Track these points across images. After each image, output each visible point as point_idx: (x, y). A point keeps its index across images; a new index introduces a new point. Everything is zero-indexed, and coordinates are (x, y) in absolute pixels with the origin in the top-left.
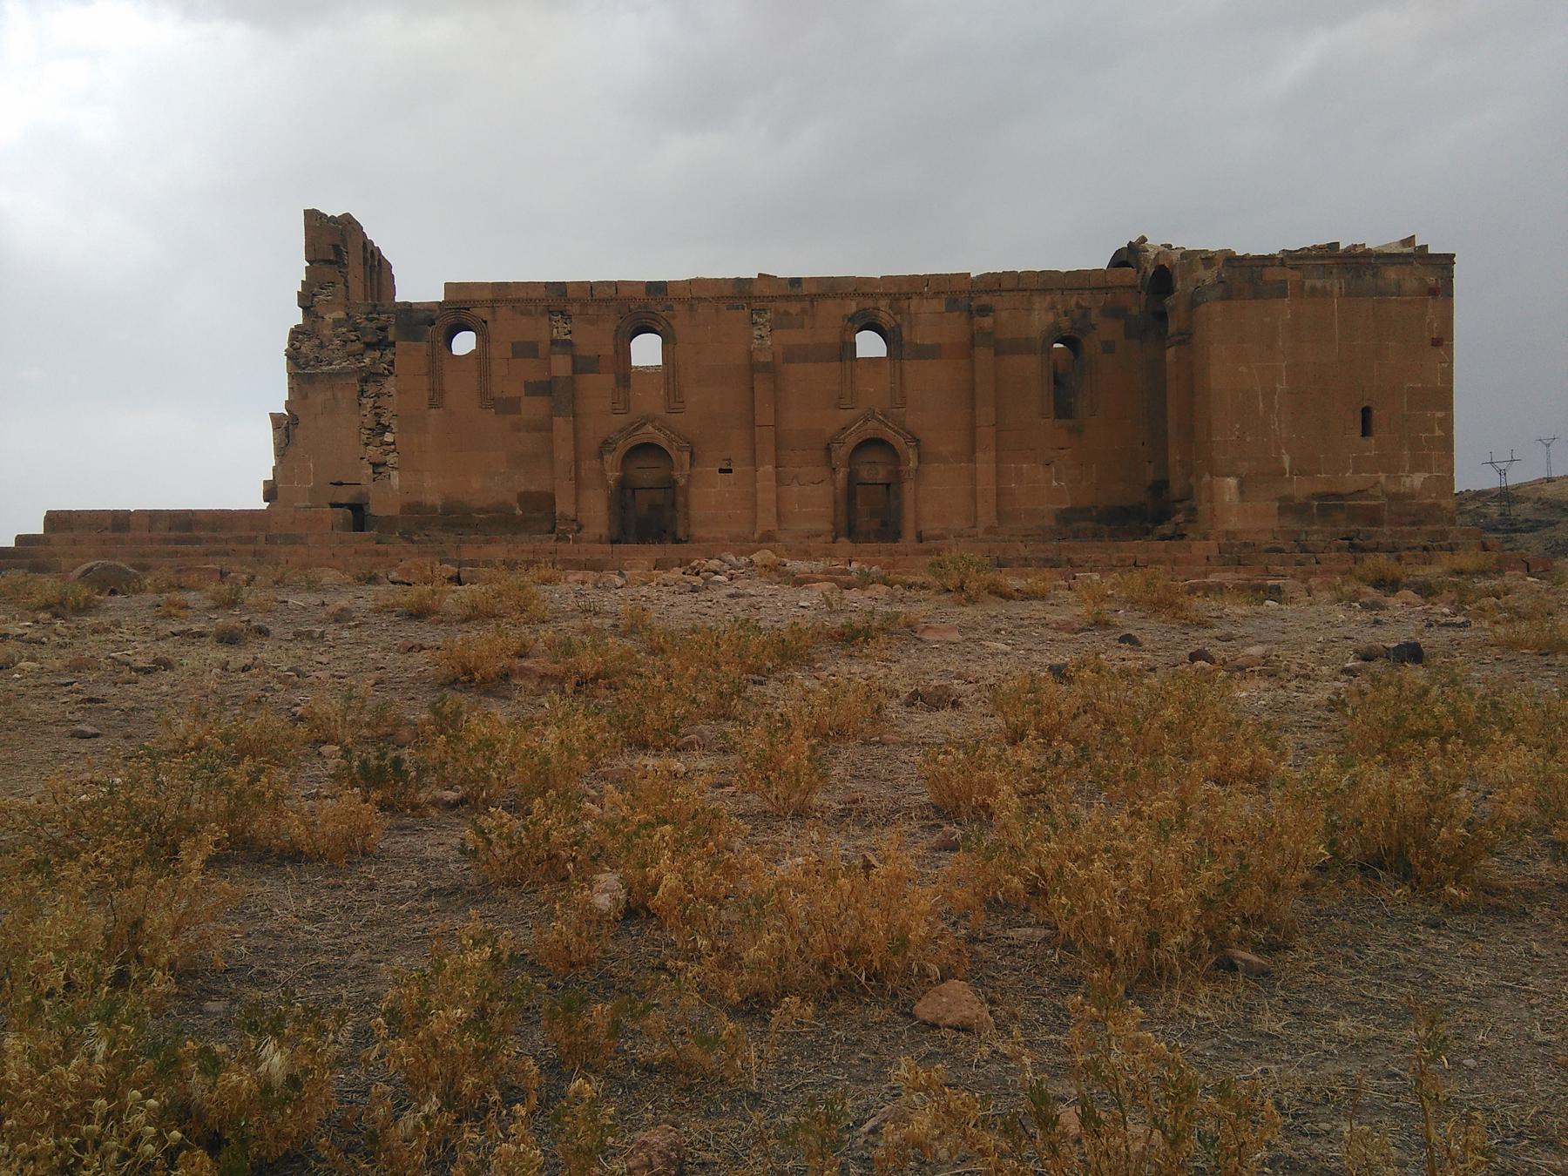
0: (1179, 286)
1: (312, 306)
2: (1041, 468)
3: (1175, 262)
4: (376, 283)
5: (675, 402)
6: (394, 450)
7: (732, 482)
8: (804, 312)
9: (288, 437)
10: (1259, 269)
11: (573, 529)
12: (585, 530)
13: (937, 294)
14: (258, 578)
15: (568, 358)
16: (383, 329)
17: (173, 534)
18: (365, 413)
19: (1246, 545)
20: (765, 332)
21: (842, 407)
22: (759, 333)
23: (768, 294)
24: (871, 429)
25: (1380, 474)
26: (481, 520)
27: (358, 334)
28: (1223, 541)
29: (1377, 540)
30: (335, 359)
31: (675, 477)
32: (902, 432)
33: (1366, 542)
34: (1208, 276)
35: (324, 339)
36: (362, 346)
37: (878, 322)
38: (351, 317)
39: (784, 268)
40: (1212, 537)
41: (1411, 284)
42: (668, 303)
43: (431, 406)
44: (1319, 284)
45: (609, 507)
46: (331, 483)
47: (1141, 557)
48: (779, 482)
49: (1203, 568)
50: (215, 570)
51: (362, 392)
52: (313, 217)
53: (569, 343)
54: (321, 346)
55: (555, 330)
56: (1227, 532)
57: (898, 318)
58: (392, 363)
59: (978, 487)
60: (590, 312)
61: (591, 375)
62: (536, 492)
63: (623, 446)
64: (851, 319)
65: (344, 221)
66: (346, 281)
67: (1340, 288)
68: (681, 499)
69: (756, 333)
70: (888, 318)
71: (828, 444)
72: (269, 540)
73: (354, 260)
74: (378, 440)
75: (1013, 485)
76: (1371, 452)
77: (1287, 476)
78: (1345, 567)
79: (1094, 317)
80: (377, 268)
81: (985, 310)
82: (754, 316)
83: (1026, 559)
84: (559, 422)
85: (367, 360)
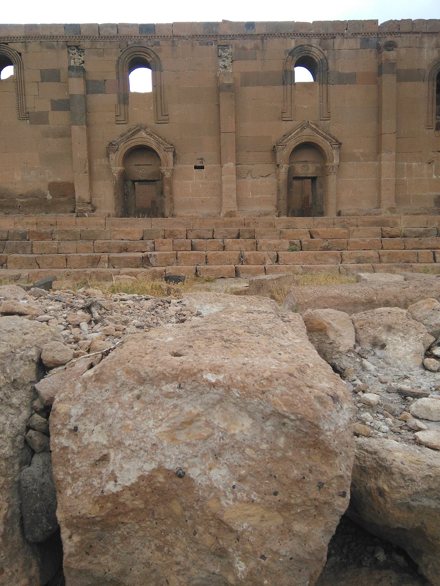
2: (425, 166)
5: (162, 115)
8: (256, 47)
11: (88, 210)
12: (98, 210)
15: (82, 81)
20: (227, 63)
21: (283, 119)
26: (22, 203)
31: (163, 171)
32: (329, 137)
37: (311, 56)
42: (156, 40)
45: (115, 194)
48: (239, 175)
55: (72, 61)
57: (325, 52)
60: (98, 46)
63: (123, 148)
68: (167, 188)
69: (221, 63)
70: (318, 52)
71: (274, 147)
75: (405, 178)
81: (391, 46)
82: (220, 50)
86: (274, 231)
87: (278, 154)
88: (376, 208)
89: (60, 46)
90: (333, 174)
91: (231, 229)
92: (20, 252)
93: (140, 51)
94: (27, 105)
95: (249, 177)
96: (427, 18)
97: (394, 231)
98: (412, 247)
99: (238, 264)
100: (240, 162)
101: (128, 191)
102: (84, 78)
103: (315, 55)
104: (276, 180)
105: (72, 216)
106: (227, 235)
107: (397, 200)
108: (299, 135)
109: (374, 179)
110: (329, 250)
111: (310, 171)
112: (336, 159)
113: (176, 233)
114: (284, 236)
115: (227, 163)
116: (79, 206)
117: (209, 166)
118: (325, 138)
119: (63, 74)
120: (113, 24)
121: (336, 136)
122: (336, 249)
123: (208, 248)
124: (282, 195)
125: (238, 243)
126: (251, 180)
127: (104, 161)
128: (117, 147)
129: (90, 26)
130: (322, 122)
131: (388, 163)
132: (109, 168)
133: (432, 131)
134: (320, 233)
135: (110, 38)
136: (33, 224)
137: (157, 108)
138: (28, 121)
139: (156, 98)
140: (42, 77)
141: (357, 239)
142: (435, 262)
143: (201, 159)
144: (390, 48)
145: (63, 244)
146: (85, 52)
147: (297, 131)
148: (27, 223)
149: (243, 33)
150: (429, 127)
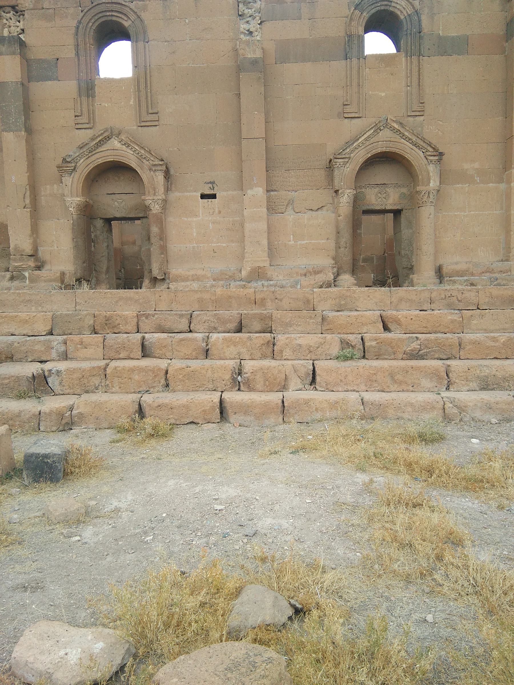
5: (148, 113)
7: (217, 211)
11: (30, 266)
12: (47, 267)
20: (253, 25)
21: (346, 115)
22: (247, 27)
31: (147, 203)
32: (422, 143)
37: (391, 9)
61: (50, 83)
68: (155, 230)
69: (243, 26)
71: (331, 161)
82: (241, 5)
86: (311, 317)
87: (336, 172)
88: (502, 261)
90: (429, 204)
93: (112, 11)
99: (231, 389)
100: (274, 188)
101: (96, 236)
102: (23, 56)
103: (398, 7)
104: (333, 215)
106: (217, 325)
108: (372, 141)
109: (498, 212)
110: (422, 357)
111: (391, 201)
112: (434, 180)
113: (117, 322)
114: (331, 326)
115: (251, 188)
116: (15, 260)
117: (225, 193)
118: (415, 145)
121: (434, 142)
122: (437, 356)
123: (175, 353)
124: (344, 240)
126: (292, 216)
128: (73, 165)
130: (411, 119)
134: (403, 320)
137: (139, 101)
141: (478, 336)
143: (210, 183)
146: (26, 16)
147: (368, 134)
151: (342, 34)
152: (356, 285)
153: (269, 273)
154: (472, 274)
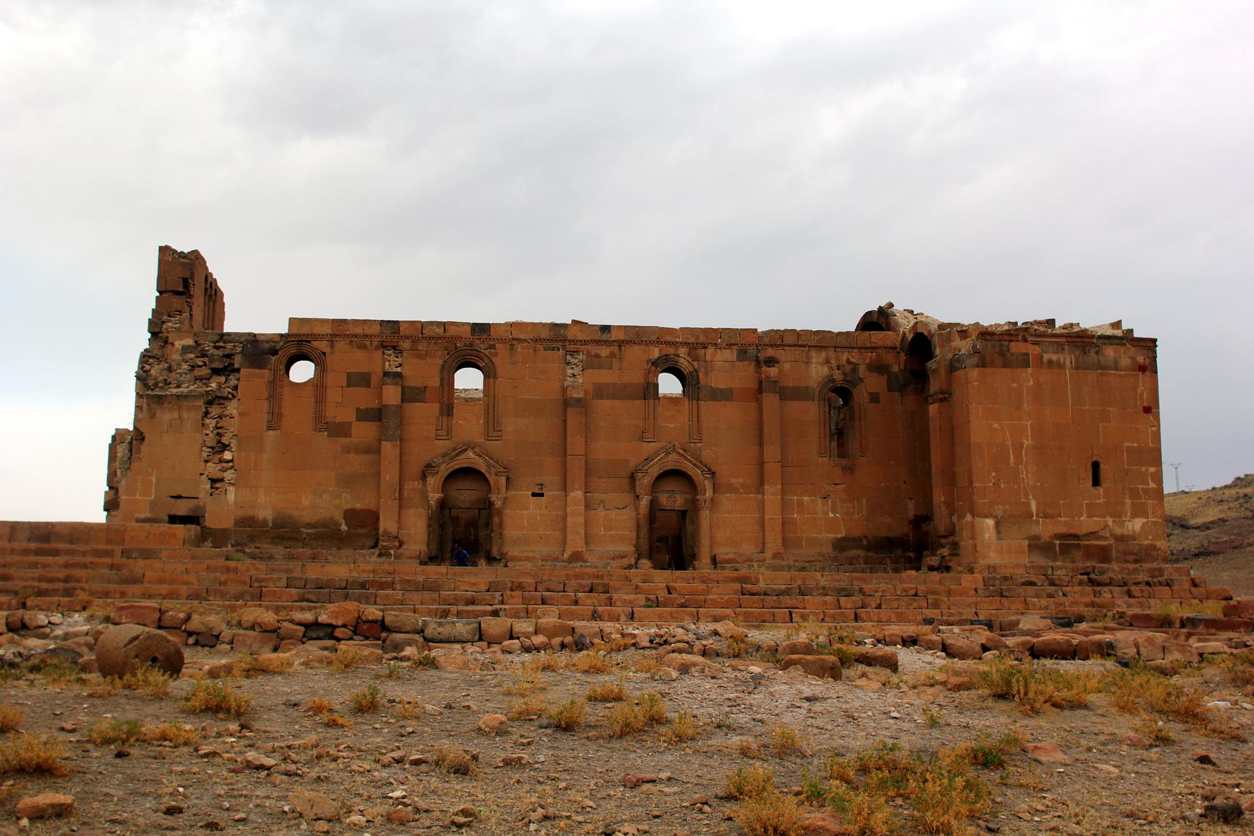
0: (937, 352)
1: (160, 332)
2: (820, 501)
3: (933, 331)
4: (211, 309)
6: (232, 467)
8: (612, 355)
9: (131, 451)
10: (1006, 343)
12: (405, 547)
13: (730, 345)
14: (195, 616)
15: (399, 389)
16: (229, 356)
17: (33, 545)
18: (207, 432)
19: (1005, 578)
20: (577, 371)
23: (581, 338)
24: (672, 461)
25: (1108, 518)
26: (308, 534)
27: (206, 360)
28: (986, 574)
29: (1109, 575)
30: (184, 382)
31: (492, 500)
32: (699, 464)
33: (1102, 577)
34: (964, 346)
35: (173, 363)
36: (209, 371)
38: (200, 345)
39: (595, 318)
40: (976, 571)
41: (1125, 362)
43: (270, 428)
44: (1054, 357)
45: (429, 526)
46: (172, 497)
47: (922, 588)
49: (974, 600)
50: (155, 609)
51: (206, 413)
52: (165, 251)
53: (399, 375)
54: (170, 369)
56: (989, 567)
57: (695, 363)
58: (236, 388)
59: (766, 517)
62: (362, 510)
63: (445, 470)
64: (655, 363)
65: (193, 257)
66: (191, 310)
67: (1071, 362)
68: (496, 520)
69: (569, 372)
71: (633, 473)
72: (126, 553)
73: (198, 291)
74: (217, 457)
76: (1099, 499)
77: (1035, 518)
78: (1087, 600)
79: (862, 368)
80: (213, 294)
81: (771, 362)
83: (824, 588)
84: (386, 445)
85: (214, 385)
87: (637, 483)
89: (374, 346)
91: (584, 582)
92: (363, 602)
94: (327, 413)
95: (601, 508)
96: (815, 329)
97: (754, 588)
98: (770, 606)
100: (590, 490)
105: (374, 554)
107: (785, 542)
108: (664, 461)
111: (678, 504)
115: (573, 491)
116: (384, 541)
118: (695, 465)
119: (375, 380)
120: (440, 322)
125: (591, 598)
127: (418, 485)
129: (412, 323)
130: (692, 445)
131: (772, 497)
132: (424, 494)
133: (826, 460)
135: (435, 339)
136: (369, 572)
137: (488, 422)
138: (326, 433)
139: (488, 410)
140: (348, 381)
142: (792, 622)
144: (771, 364)
145: (408, 595)
146: (404, 355)
148: (364, 571)
149: (596, 338)
150: (821, 455)
151: (642, 381)
152: (652, 568)
153: (586, 557)
154: (738, 563)
